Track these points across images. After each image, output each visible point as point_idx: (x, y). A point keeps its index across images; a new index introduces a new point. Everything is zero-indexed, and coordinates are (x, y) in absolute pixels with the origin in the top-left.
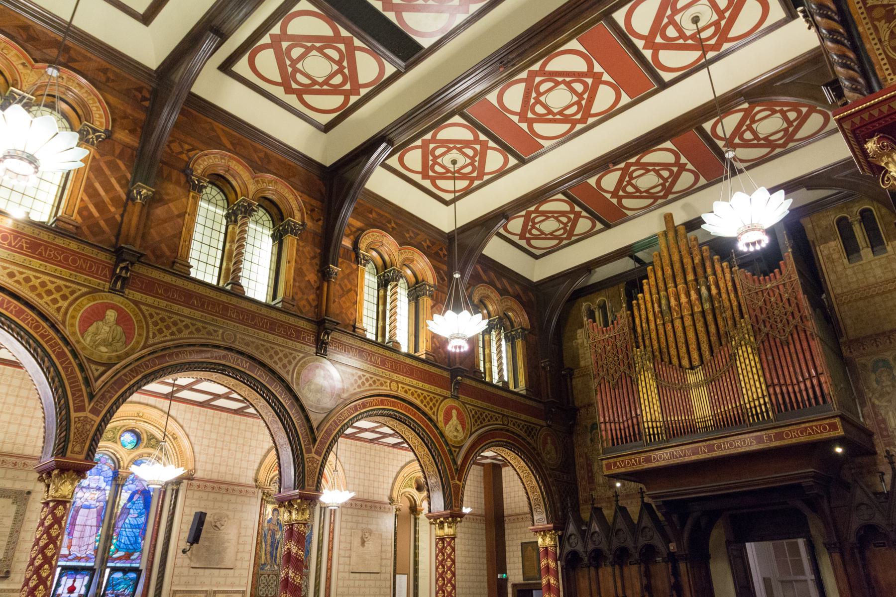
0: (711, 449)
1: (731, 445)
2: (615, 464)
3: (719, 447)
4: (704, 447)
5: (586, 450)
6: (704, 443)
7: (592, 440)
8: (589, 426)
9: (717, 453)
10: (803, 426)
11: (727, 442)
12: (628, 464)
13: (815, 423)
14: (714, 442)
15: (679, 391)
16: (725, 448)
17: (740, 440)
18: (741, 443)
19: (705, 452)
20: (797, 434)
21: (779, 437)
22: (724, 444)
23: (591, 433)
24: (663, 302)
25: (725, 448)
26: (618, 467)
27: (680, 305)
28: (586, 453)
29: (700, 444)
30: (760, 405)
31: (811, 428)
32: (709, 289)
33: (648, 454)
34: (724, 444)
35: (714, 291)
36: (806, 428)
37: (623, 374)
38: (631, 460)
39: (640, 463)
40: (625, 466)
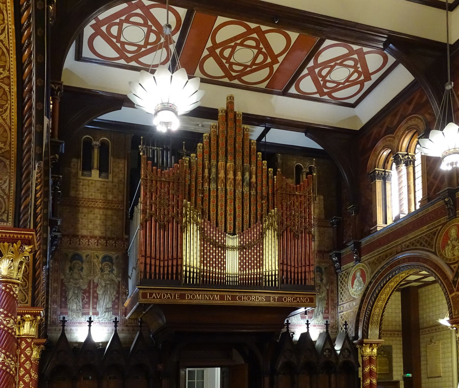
0: (234, 298)
1: (249, 299)
2: (151, 295)
3: (240, 298)
4: (229, 296)
5: (63, 277)
6: (230, 294)
7: (71, 269)
8: (70, 255)
9: (238, 302)
10: (295, 296)
11: (246, 296)
12: (164, 296)
13: (302, 296)
14: (237, 294)
16: (244, 299)
17: (255, 296)
18: (255, 299)
19: (229, 300)
20: (291, 300)
22: (244, 297)
23: (71, 262)
25: (244, 299)
26: (154, 297)
28: (62, 280)
29: (227, 293)
31: (300, 298)
34: (244, 297)
36: (297, 298)
38: (167, 294)
39: (175, 298)
40: (160, 298)
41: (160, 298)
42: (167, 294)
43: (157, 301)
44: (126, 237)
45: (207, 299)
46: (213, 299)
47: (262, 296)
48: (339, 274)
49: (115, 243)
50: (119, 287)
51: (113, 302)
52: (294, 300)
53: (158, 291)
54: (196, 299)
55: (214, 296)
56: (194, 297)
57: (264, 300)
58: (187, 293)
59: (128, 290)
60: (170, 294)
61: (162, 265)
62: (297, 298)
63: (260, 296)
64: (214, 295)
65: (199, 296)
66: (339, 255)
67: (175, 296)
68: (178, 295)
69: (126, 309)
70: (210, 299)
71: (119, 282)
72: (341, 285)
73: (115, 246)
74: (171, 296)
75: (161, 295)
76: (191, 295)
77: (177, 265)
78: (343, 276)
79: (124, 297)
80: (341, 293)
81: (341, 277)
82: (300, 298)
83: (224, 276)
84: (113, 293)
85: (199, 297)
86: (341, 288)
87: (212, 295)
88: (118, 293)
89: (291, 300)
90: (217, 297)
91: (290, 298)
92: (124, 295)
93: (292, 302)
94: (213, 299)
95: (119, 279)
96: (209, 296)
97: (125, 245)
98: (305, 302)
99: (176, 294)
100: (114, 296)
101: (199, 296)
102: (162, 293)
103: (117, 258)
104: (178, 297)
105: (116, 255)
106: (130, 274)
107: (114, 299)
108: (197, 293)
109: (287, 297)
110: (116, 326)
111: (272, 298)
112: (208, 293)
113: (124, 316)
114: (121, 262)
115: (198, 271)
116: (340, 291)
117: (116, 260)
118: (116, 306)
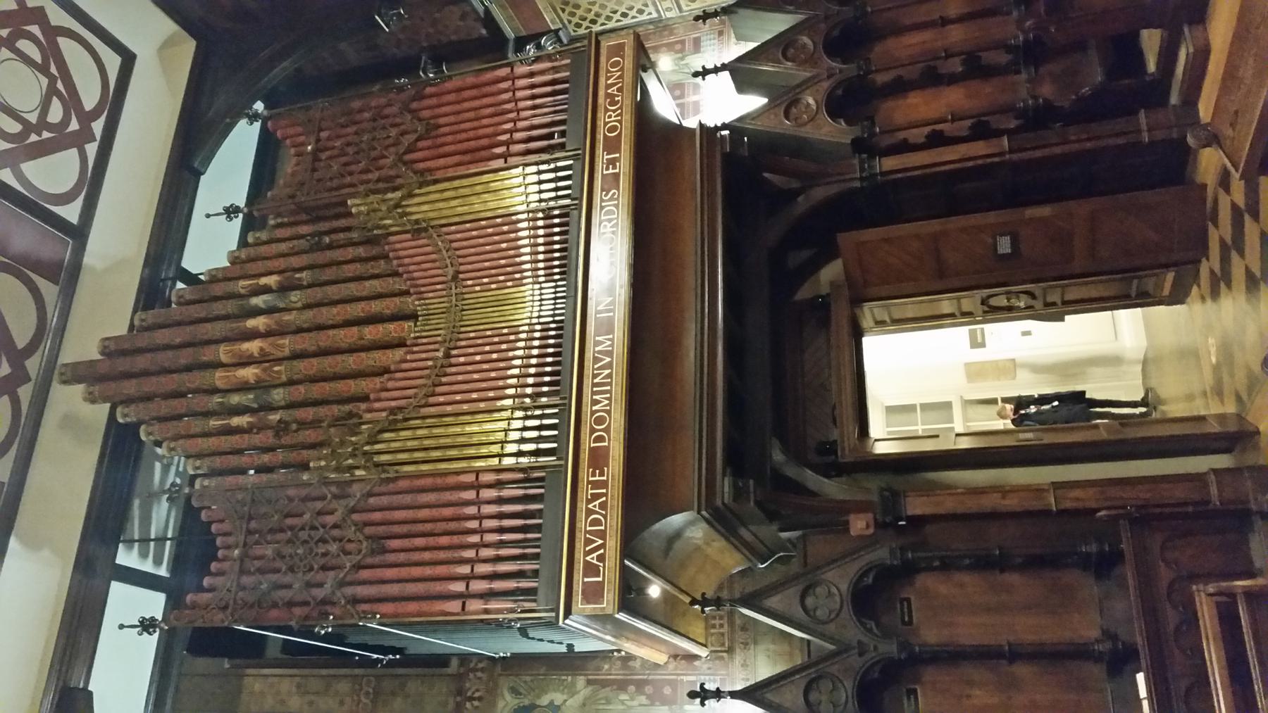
2: (591, 569)
10: (601, 100)
12: (596, 522)
15: (453, 360)
20: (614, 111)
21: (613, 146)
24: (235, 399)
27: (259, 359)
30: (540, 182)
31: (608, 86)
32: (266, 290)
33: (585, 456)
35: (272, 280)
36: (608, 95)
37: (355, 517)
39: (604, 484)
41: (602, 534)
42: (590, 512)
43: (613, 544)
44: (455, 662)
45: (609, 376)
46: (609, 354)
47: (602, 201)
48: (573, 34)
49: (471, 699)
50: (604, 684)
51: (652, 705)
52: (615, 103)
53: (580, 545)
54: (609, 412)
55: (599, 352)
56: (600, 421)
57: (614, 194)
58: (587, 443)
59: (612, 651)
60: (589, 502)
61: (494, 537)
62: (608, 95)
63: (602, 208)
64: (594, 352)
65: (597, 402)
66: (521, 43)
67: (596, 485)
68: (594, 475)
69: (675, 657)
70: (609, 365)
71: (589, 682)
72: (601, 20)
73: (480, 699)
74: (595, 497)
75: (590, 532)
76: (593, 431)
77: (499, 484)
78: (575, 20)
79: (637, 664)
80: (624, 15)
81: (578, 25)
82: (608, 86)
83: (538, 327)
84: (622, 702)
85: (600, 402)
86: (609, 18)
87: (596, 360)
88: (622, 686)
89: (614, 111)
90: (601, 343)
91: (610, 117)
92: (631, 663)
93: (621, 108)
94: (609, 354)
95: (581, 681)
96: (599, 369)
97: (480, 665)
98: (622, 69)
99: (589, 482)
100: (632, 699)
101: (597, 402)
102: (586, 532)
103: (515, 691)
104: (602, 474)
105: (508, 697)
106: (563, 649)
107: (643, 699)
108: (587, 409)
109: (606, 124)
110: (718, 694)
111: (607, 169)
112: (588, 372)
113: (697, 663)
114: (528, 678)
115: (519, 414)
116: (618, 21)
117: (521, 694)
118: (667, 691)
